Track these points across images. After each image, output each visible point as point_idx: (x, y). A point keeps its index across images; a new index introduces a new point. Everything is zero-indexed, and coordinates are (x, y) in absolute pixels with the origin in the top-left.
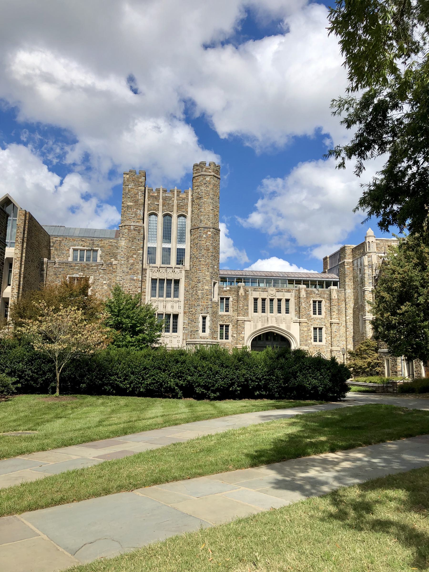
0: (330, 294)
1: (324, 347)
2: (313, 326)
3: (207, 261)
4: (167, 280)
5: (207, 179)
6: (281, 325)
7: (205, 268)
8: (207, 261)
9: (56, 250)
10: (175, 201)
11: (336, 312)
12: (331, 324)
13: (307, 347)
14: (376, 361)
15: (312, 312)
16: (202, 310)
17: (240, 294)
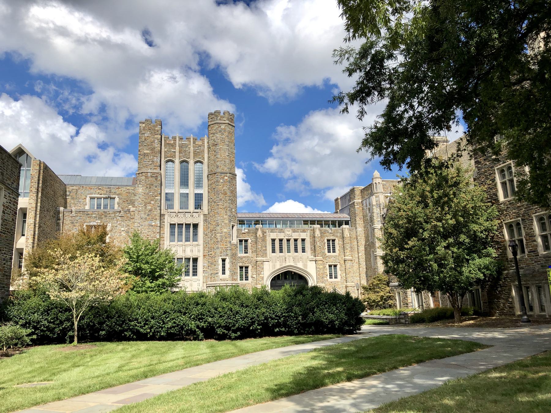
0: (343, 233)
3: (225, 204)
4: (186, 224)
5: (222, 127)
6: (298, 264)
7: (223, 212)
8: (225, 204)
9: (73, 199)
10: (192, 148)
11: (349, 249)
14: (388, 294)
16: (221, 253)
17: (258, 236)
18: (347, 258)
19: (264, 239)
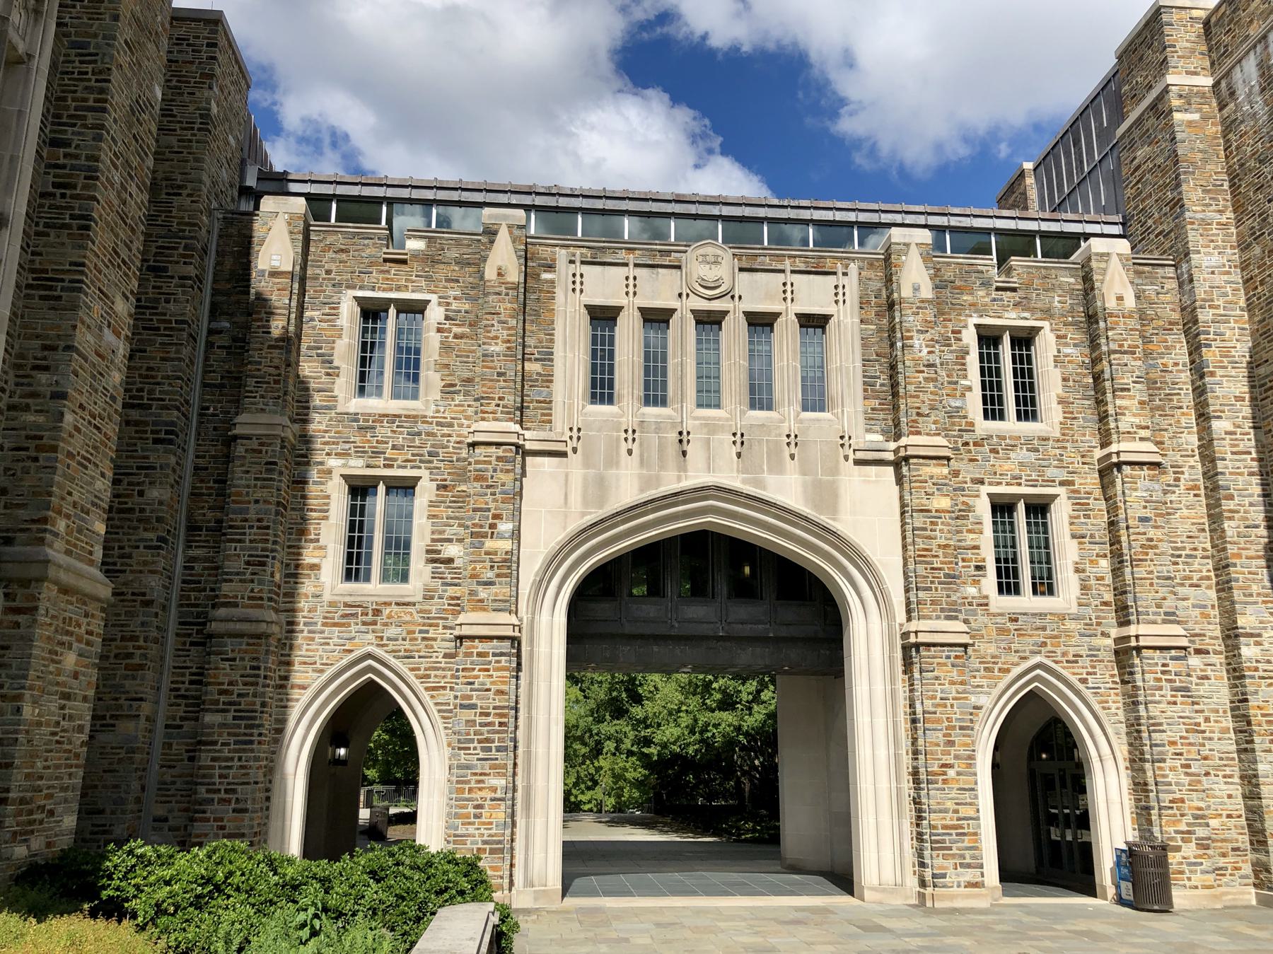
1: (1070, 625)
2: (985, 490)
6: (771, 479)
11: (1139, 391)
12: (1108, 470)
13: (959, 626)
15: (974, 404)
17: (490, 273)
18: (1124, 448)
19: (531, 296)
